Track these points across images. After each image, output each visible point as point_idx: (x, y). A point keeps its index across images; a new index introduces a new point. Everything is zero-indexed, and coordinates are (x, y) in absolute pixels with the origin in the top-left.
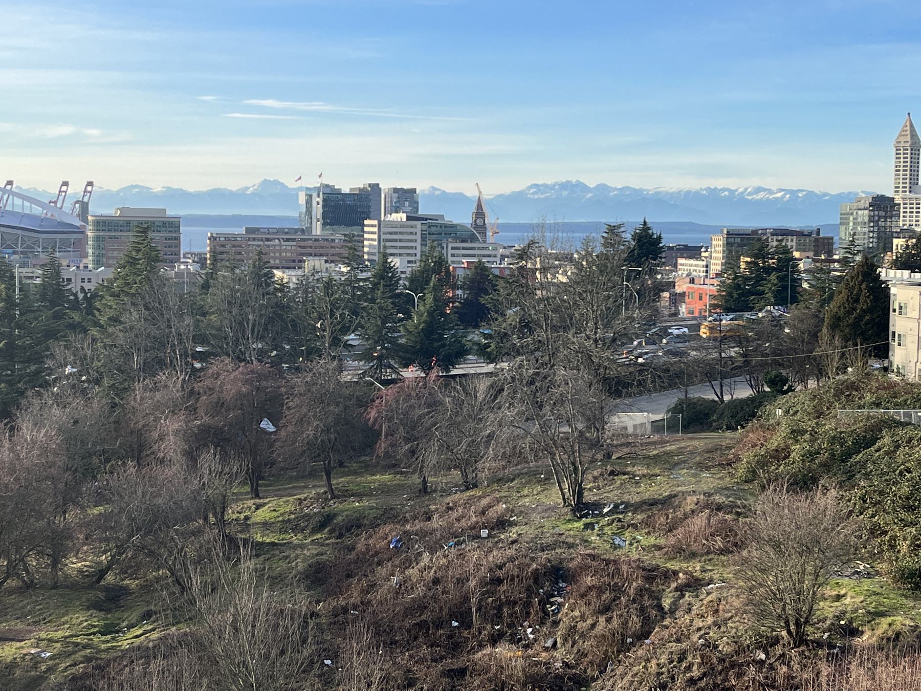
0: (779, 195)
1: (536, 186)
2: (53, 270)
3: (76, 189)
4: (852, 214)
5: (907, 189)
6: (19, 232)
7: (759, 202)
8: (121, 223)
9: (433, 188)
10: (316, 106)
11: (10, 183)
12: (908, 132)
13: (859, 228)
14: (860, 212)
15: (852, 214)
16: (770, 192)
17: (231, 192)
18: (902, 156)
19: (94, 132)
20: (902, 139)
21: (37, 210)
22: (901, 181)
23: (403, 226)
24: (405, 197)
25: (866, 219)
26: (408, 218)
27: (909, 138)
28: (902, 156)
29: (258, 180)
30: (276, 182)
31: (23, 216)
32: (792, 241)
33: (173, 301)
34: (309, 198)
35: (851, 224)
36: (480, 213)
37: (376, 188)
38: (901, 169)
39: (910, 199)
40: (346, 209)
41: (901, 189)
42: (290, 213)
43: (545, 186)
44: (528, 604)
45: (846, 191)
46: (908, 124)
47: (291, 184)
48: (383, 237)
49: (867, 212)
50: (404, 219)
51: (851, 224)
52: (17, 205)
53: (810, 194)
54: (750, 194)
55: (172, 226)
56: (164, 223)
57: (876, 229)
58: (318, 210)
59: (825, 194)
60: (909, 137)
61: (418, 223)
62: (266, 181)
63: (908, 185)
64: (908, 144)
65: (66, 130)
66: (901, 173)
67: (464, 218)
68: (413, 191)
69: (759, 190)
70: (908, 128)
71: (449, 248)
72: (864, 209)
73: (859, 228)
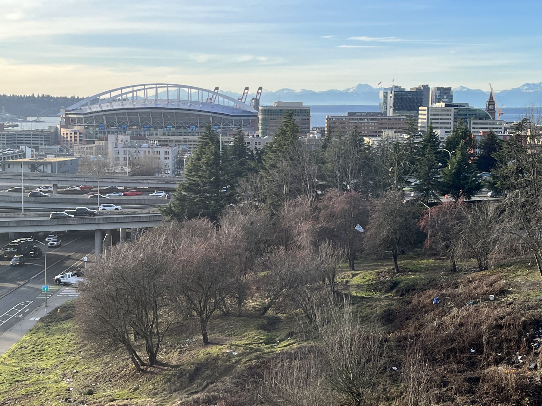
1: (528, 84)
2: (240, 138)
3: (252, 91)
6: (221, 116)
8: (277, 111)
9: (462, 86)
11: (217, 88)
17: (340, 92)
19: (263, 58)
21: (232, 104)
23: (442, 110)
24: (444, 93)
26: (446, 106)
29: (356, 84)
30: (366, 86)
31: (224, 107)
33: (306, 156)
34: (386, 94)
36: (491, 102)
37: (426, 87)
40: (408, 101)
42: (374, 104)
43: (534, 84)
44: (519, 341)
47: (375, 86)
48: (430, 117)
50: (444, 106)
52: (220, 101)
55: (306, 112)
56: (301, 110)
58: (391, 101)
61: (452, 108)
62: (360, 85)
65: (247, 58)
67: (481, 105)
68: (449, 89)
71: (472, 124)
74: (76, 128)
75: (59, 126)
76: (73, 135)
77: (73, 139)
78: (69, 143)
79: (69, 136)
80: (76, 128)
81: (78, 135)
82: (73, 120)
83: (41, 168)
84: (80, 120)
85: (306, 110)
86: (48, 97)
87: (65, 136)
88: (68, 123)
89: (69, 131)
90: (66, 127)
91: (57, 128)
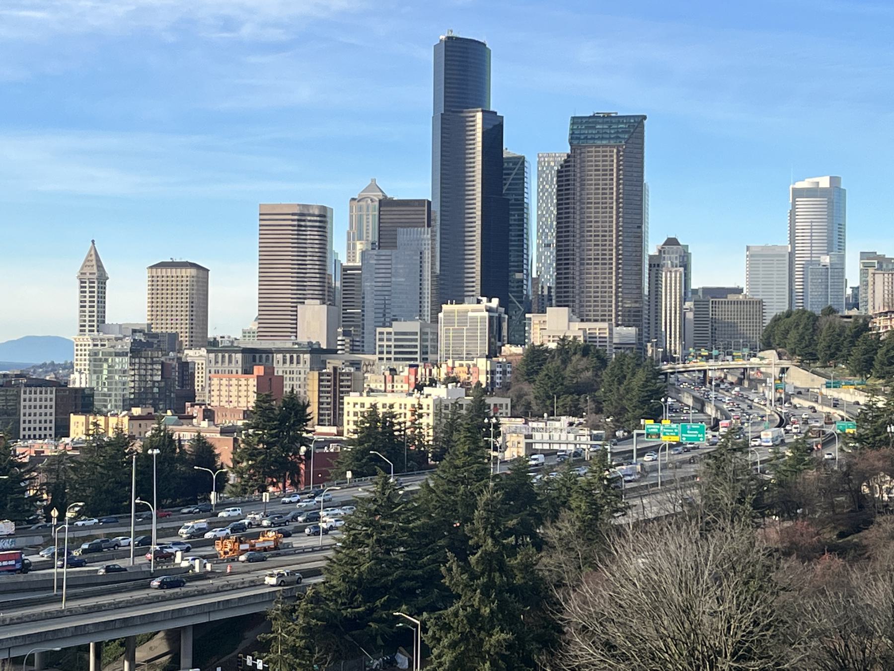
4: (106, 360)
5: (95, 328)
12: (94, 263)
13: (117, 377)
14: (117, 360)
15: (106, 360)
18: (87, 290)
20: (87, 270)
22: (87, 319)
25: (126, 367)
27: (95, 270)
28: (87, 290)
32: (51, 393)
35: (105, 372)
38: (87, 304)
39: (101, 340)
41: (87, 328)
46: (93, 252)
49: (126, 359)
51: (105, 372)
57: (137, 378)
60: (95, 267)
63: (95, 324)
64: (95, 276)
66: (87, 309)
70: (93, 257)
72: (124, 354)
73: (117, 377)
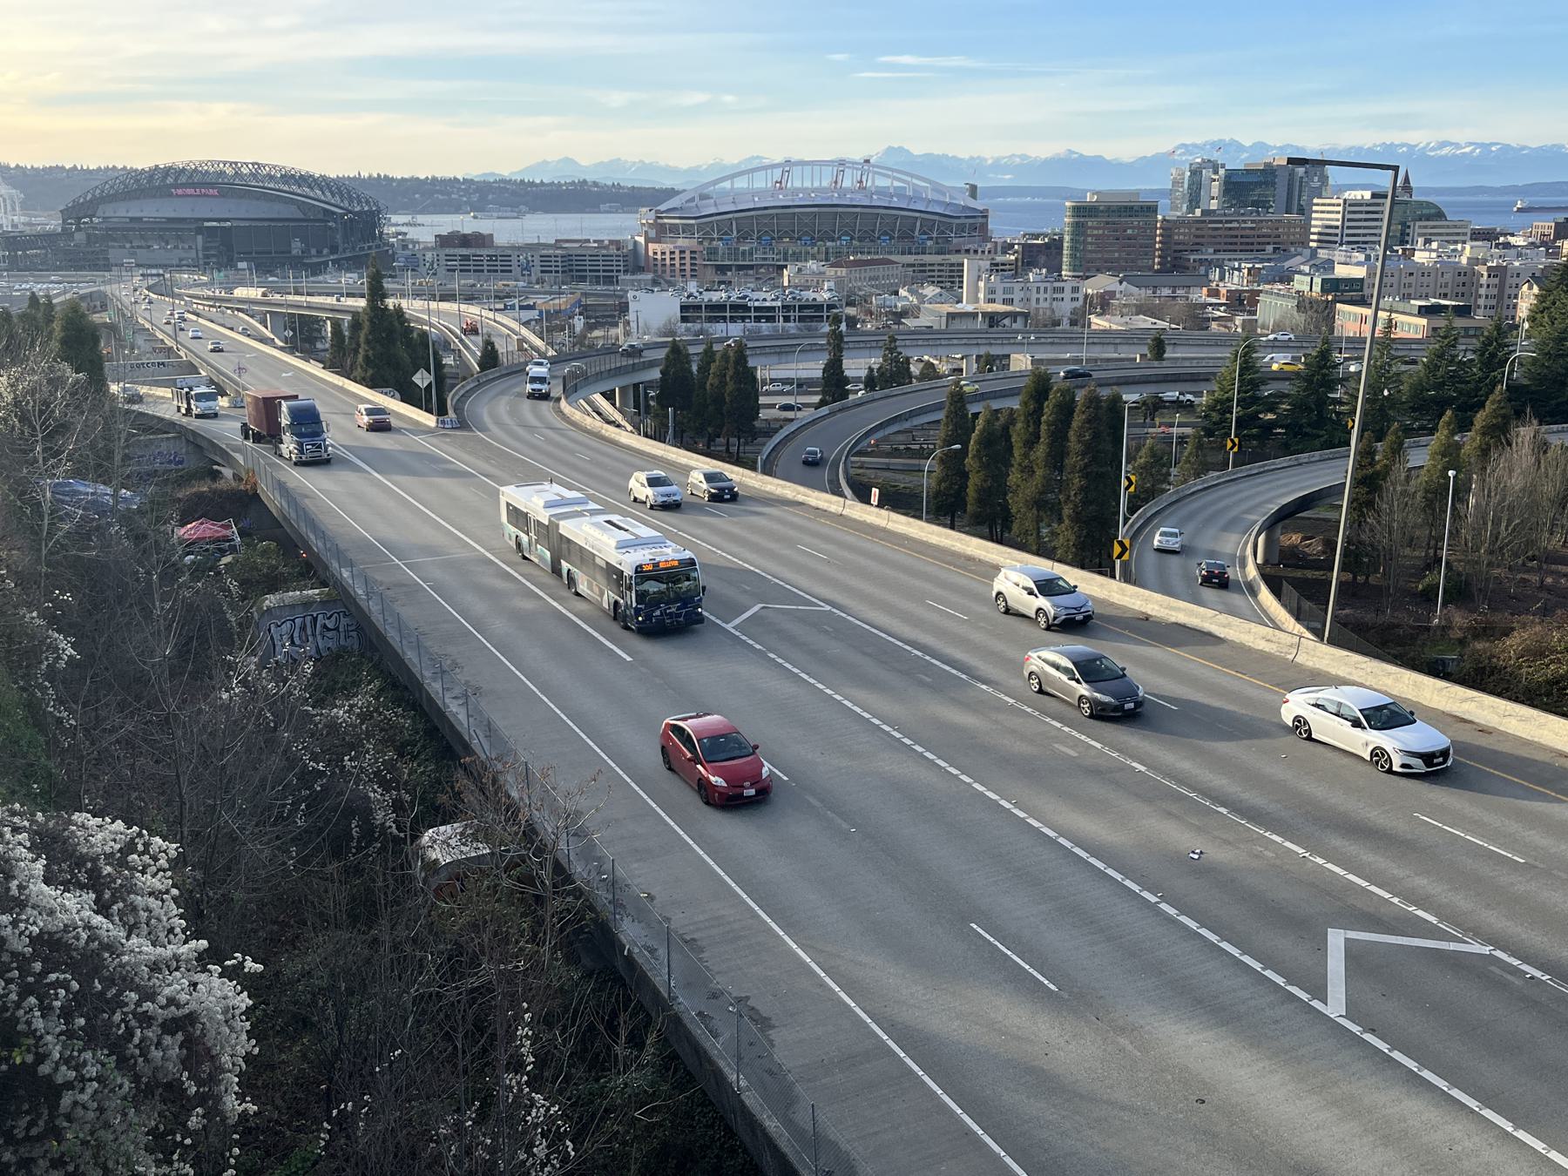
0: (1467, 150)
1: (1184, 145)
7: (1442, 158)
10: (956, 61)
16: (1457, 146)
19: (729, 98)
26: (1374, 196)
29: (882, 148)
30: (901, 149)
43: (1195, 146)
45: (1550, 144)
53: (1506, 148)
54: (1433, 149)
55: (1152, 209)
59: (1524, 148)
62: (890, 149)
65: (700, 97)
69: (1443, 144)
74: (681, 242)
75: (641, 240)
76: (677, 256)
77: (677, 262)
78: (668, 269)
79: (667, 256)
80: (681, 242)
81: (687, 255)
82: (674, 229)
83: (1007, 321)
84: (686, 228)
85: (1149, 208)
86: (434, 179)
87: (659, 257)
88: (660, 231)
89: (667, 247)
90: (657, 240)
91: (636, 243)
